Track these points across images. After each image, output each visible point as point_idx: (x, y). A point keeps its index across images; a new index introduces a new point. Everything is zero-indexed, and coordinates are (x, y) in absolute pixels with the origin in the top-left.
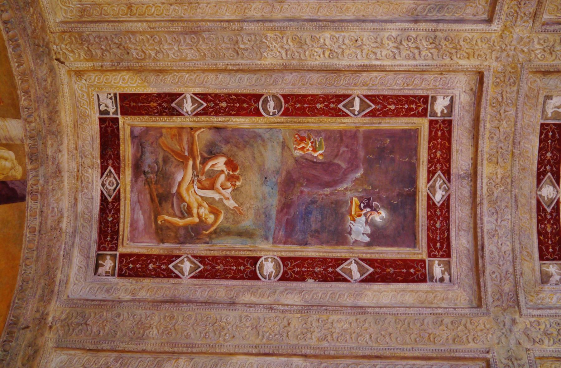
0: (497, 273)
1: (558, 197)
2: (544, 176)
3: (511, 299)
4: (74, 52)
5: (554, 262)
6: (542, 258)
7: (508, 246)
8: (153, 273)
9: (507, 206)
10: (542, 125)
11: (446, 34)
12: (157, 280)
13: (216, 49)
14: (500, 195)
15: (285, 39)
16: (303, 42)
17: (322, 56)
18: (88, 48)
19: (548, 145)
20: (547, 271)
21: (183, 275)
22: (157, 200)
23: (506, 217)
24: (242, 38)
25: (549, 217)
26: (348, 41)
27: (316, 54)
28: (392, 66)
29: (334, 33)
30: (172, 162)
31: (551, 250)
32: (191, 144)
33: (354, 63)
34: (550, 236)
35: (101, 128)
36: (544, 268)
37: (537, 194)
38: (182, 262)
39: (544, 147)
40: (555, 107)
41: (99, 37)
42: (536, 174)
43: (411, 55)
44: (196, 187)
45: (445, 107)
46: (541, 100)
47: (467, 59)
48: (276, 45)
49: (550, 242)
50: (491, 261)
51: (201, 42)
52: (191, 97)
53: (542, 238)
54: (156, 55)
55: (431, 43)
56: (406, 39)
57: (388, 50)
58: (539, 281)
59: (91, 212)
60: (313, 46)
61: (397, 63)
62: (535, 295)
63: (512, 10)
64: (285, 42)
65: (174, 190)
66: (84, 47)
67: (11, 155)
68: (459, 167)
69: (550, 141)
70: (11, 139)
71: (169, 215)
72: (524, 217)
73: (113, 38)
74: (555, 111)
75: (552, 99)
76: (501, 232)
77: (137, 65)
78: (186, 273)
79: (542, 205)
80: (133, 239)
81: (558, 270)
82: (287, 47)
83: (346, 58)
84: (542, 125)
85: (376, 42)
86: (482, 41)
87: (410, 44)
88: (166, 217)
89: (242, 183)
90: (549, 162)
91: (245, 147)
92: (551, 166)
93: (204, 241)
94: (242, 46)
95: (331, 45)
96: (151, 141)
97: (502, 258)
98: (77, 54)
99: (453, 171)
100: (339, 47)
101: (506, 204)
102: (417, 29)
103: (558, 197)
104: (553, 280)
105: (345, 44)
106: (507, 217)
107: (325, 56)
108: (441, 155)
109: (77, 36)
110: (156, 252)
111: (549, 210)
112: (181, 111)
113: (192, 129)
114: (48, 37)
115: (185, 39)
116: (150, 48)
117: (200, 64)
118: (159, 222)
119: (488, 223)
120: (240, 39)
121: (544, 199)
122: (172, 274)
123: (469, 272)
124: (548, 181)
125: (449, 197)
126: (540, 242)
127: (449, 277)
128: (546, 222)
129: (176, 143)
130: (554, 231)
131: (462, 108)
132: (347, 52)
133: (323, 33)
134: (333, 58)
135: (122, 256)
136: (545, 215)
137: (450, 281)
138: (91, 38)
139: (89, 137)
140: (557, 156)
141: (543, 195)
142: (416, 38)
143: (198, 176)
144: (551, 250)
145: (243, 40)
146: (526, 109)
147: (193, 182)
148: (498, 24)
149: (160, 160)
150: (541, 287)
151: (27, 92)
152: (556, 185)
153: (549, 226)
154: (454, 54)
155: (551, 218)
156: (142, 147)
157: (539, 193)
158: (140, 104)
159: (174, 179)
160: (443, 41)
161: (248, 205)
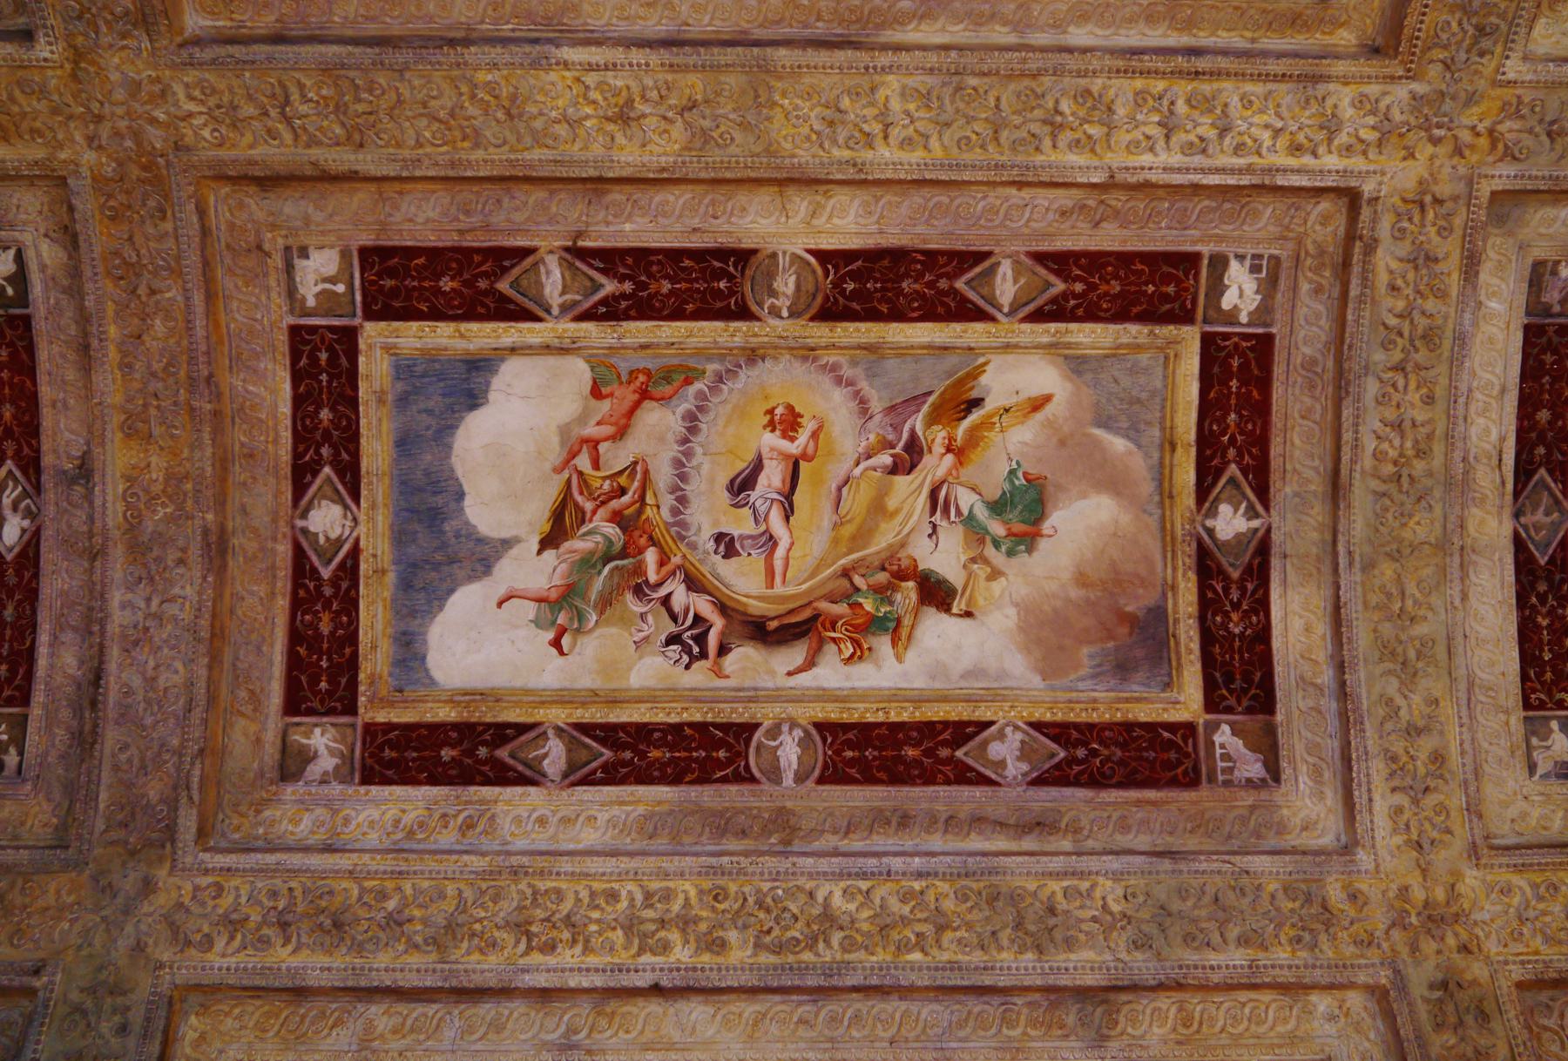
0: (133, 751)
1: (355, 534)
2: (315, 473)
3: (159, 821)
5: (325, 719)
6: (294, 704)
7: (176, 672)
9: (181, 562)
10: (295, 331)
14: (161, 528)
19: (321, 389)
20: (303, 745)
23: (176, 591)
25: (328, 591)
31: (323, 685)
34: (325, 646)
36: (297, 737)
37: (293, 527)
39: (309, 393)
40: (325, 280)
42: (288, 470)
45: (5, 279)
46: (278, 260)
49: (324, 664)
50: (122, 715)
53: (302, 651)
58: (272, 774)
62: (251, 813)
68: (61, 450)
69: (324, 377)
72: (252, 593)
74: (324, 292)
75: (307, 257)
76: (160, 635)
79: (308, 559)
81: (335, 741)
84: (295, 331)
90: (327, 436)
92: (333, 446)
97: (156, 708)
99: (47, 460)
101: (180, 554)
103: (355, 534)
104: (315, 770)
106: (182, 593)
108: (14, 417)
111: (326, 573)
119: (123, 607)
121: (317, 541)
123: (70, 747)
124: (328, 490)
125: (37, 534)
126: (294, 663)
127: (17, 759)
128: (319, 607)
130: (341, 632)
131: (51, 284)
136: (318, 588)
137: (19, 771)
140: (348, 419)
141: (312, 529)
144: (323, 685)
146: (236, 286)
150: (274, 788)
152: (349, 501)
153: (326, 617)
155: (335, 595)
157: (300, 523)
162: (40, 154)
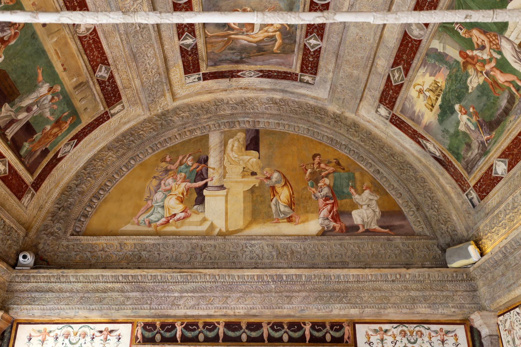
8: (316, 59)
12: (321, 59)
21: (319, 44)
22: (261, 53)
30: (232, 46)
32: (218, 36)
35: (210, 79)
38: (310, 44)
44: (252, 33)
48: (132, 9)
52: (182, 41)
59: (270, 83)
65: (255, 45)
67: (230, 141)
70: (221, 142)
71: (274, 47)
78: (318, 43)
80: (291, 66)
88: (275, 48)
89: (249, 7)
91: (218, 6)
93: (295, 30)
96: (217, 57)
110: (301, 57)
112: (193, 45)
113: (206, 38)
118: (279, 52)
122: (318, 50)
129: (218, 44)
135: (302, 71)
139: (217, 84)
143: (243, 32)
147: (248, 35)
149: (232, 52)
151: (191, 132)
156: (223, 60)
158: (191, 64)
159: (246, 45)
161: (267, 4)
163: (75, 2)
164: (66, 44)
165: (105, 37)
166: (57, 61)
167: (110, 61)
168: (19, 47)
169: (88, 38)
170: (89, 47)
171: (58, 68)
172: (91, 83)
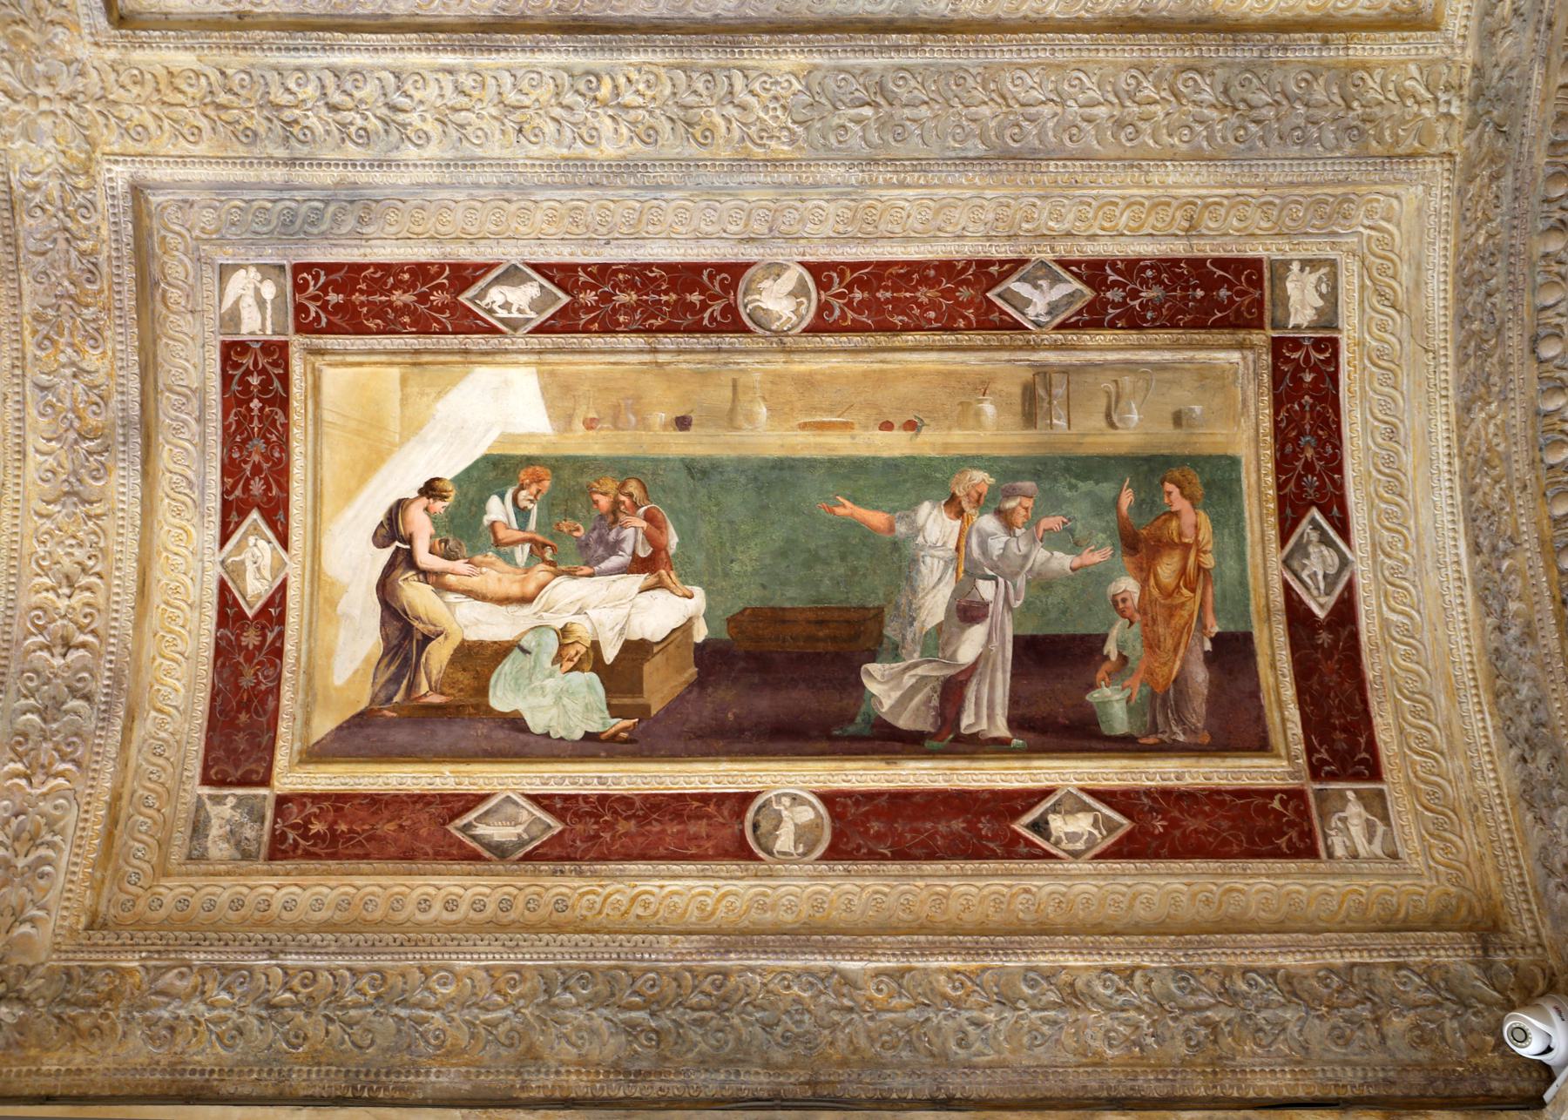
4: (1398, 94)
11: (256, 151)
13: (947, 100)
15: (736, 134)
16: (680, 125)
17: (622, 81)
18: (1349, 107)
24: (864, 138)
26: (546, 130)
27: (641, 87)
28: (401, 49)
29: (590, 152)
33: (521, 59)
41: (1304, 141)
43: (348, 86)
47: (175, 70)
48: (762, 114)
51: (993, 124)
54: (1139, 83)
55: (296, 121)
56: (373, 138)
57: (421, 102)
60: (651, 112)
61: (387, 59)
63: (84, 222)
64: (735, 125)
66: (1360, 111)
73: (1262, 138)
77: (1211, 50)
82: (731, 111)
83: (545, 73)
85: (462, 126)
86: (145, 128)
87: (359, 122)
94: (867, 111)
95: (596, 115)
98: (1391, 86)
100: (569, 108)
102: (345, 165)
105: (554, 119)
107: (613, 79)
109: (1374, 143)
114: (1465, 143)
115: (1041, 136)
116: (1153, 108)
117: (1004, 53)
120: (874, 138)
132: (545, 93)
133: (621, 152)
134: (588, 73)
138: (1330, 137)
142: (343, 140)
145: (864, 130)
148: (111, 179)
154: (216, 88)
160: (262, 131)
162: (138, 56)
163: (664, 298)
164: (808, 383)
165: (866, 240)
166: (853, 437)
167: (1001, 251)
168: (705, 529)
169: (836, 303)
170: (881, 311)
171: (895, 445)
172: (1052, 357)
